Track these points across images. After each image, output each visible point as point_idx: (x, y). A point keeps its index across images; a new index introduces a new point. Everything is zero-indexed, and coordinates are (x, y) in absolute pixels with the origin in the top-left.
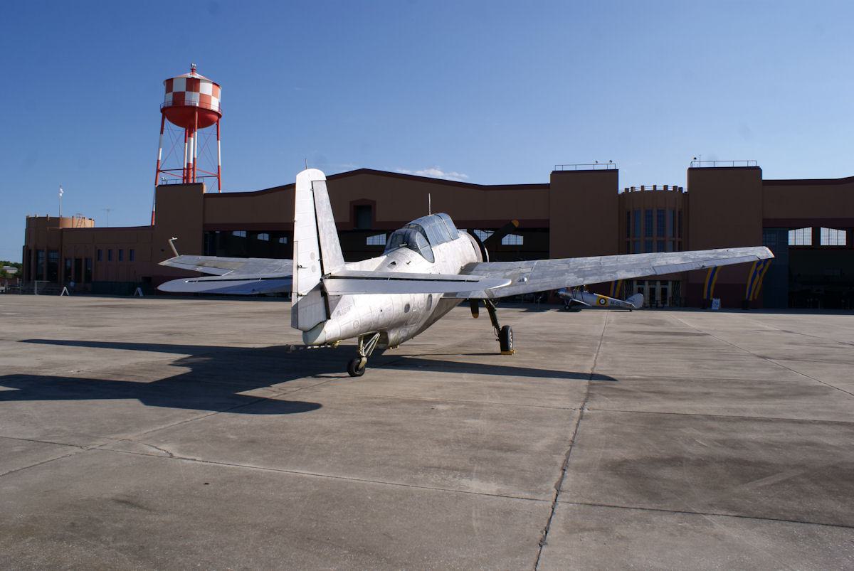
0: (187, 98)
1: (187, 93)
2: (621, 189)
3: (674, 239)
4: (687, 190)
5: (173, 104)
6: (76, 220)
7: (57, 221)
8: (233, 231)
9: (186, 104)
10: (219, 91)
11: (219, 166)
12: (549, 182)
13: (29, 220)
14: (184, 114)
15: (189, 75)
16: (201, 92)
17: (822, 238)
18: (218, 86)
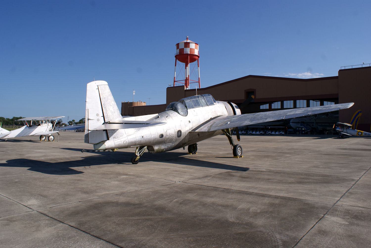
0: (185, 51)
1: (185, 49)
5: (179, 54)
6: (139, 103)
7: (131, 103)
9: (185, 53)
10: (198, 46)
11: (199, 78)
12: (338, 75)
13: (122, 103)
14: (185, 57)
15: (185, 41)
18: (197, 44)
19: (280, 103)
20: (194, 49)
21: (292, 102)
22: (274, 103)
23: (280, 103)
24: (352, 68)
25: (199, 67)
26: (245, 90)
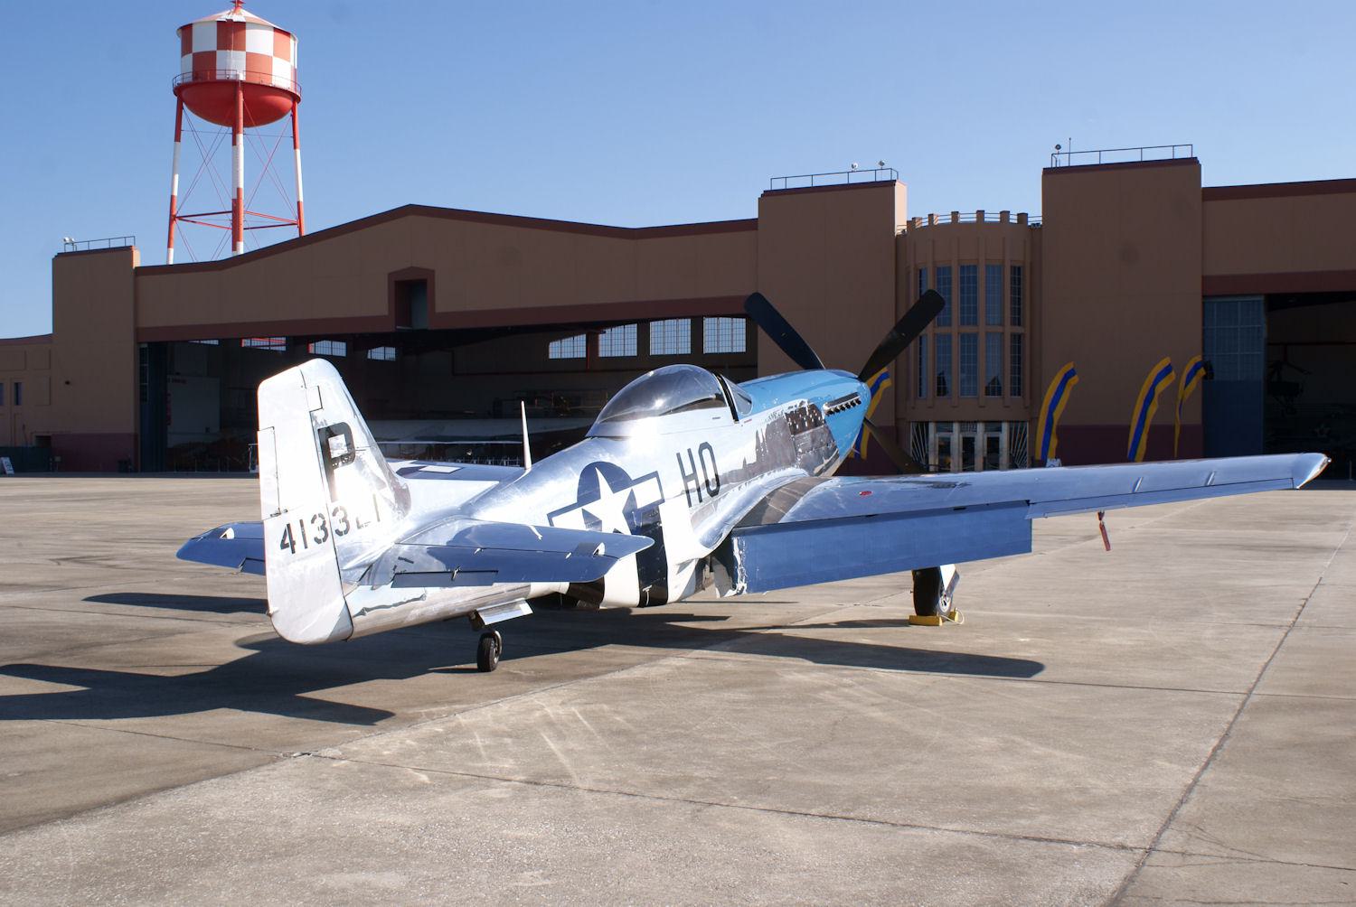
0: (219, 66)
1: (219, 53)
2: (900, 224)
3: (1000, 329)
4: (1039, 220)
5: (196, 74)
8: (241, 339)
9: (218, 77)
10: (293, 44)
11: (298, 203)
12: (757, 217)
14: (217, 97)
15: (224, 16)
16: (249, 49)
17: (705, 339)
18: (288, 34)
19: (632, 330)
20: (268, 60)
21: (685, 324)
22: (608, 331)
23: (632, 330)
24: (846, 182)
25: (298, 151)
26: (390, 275)
